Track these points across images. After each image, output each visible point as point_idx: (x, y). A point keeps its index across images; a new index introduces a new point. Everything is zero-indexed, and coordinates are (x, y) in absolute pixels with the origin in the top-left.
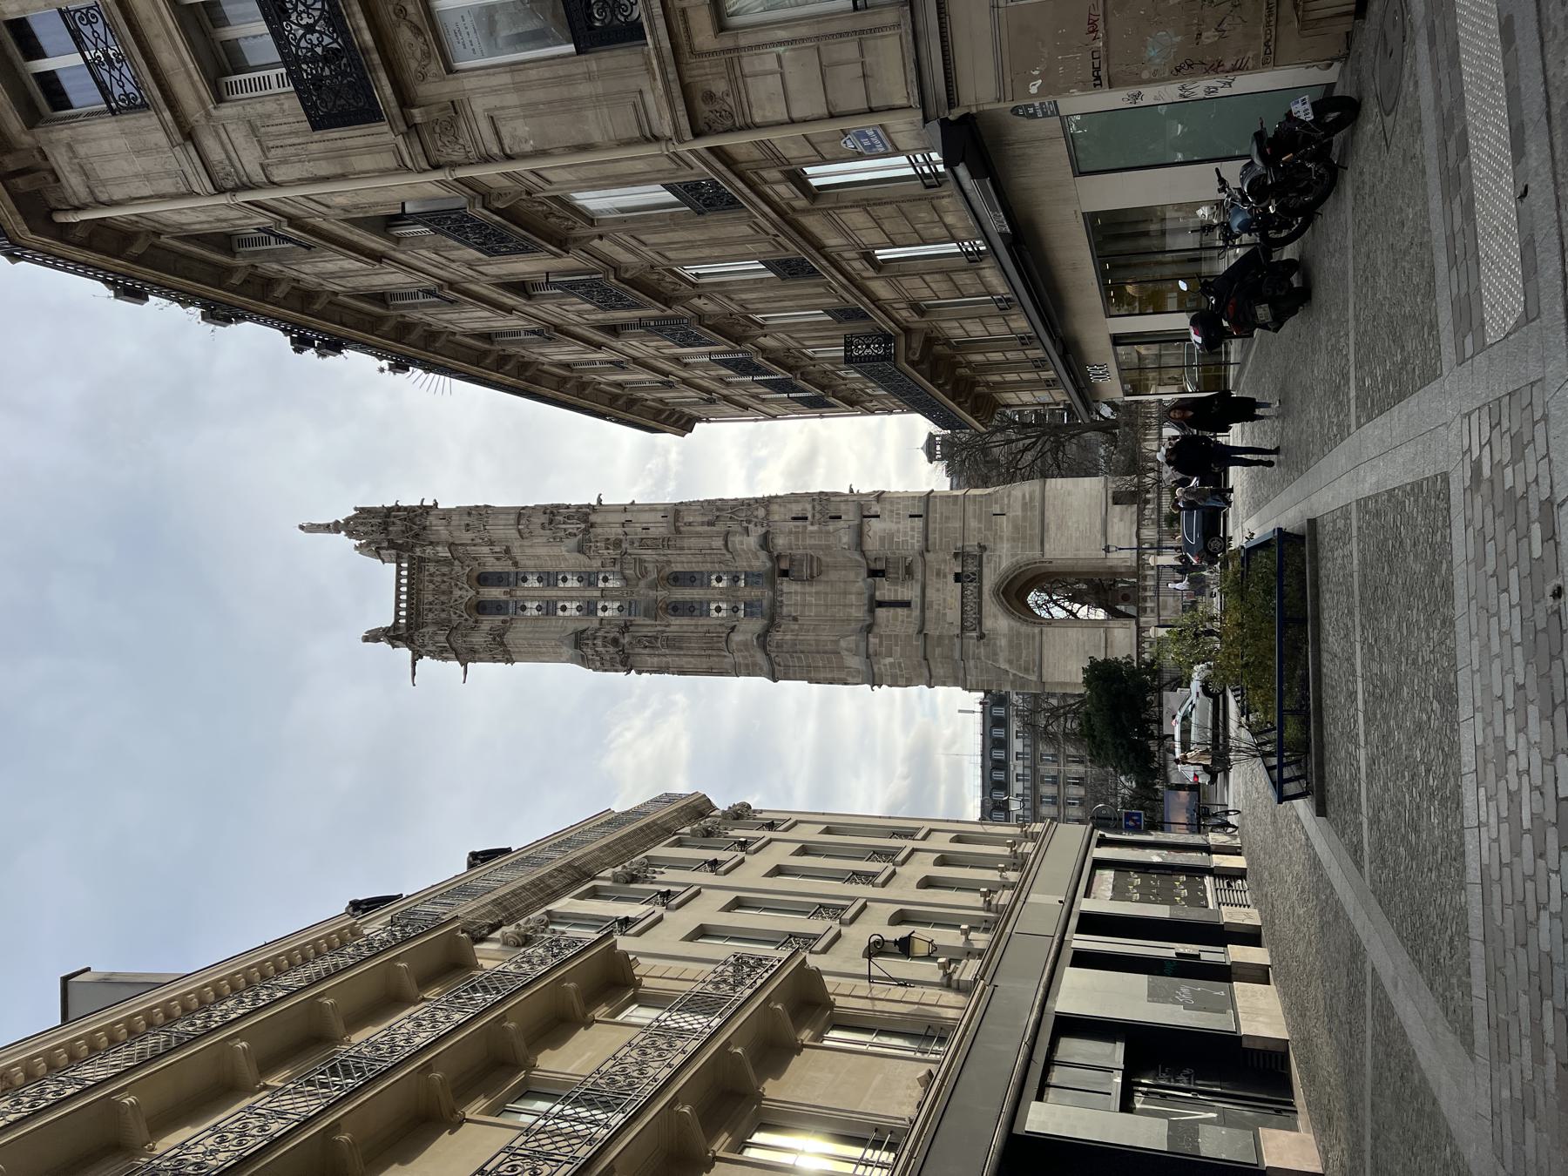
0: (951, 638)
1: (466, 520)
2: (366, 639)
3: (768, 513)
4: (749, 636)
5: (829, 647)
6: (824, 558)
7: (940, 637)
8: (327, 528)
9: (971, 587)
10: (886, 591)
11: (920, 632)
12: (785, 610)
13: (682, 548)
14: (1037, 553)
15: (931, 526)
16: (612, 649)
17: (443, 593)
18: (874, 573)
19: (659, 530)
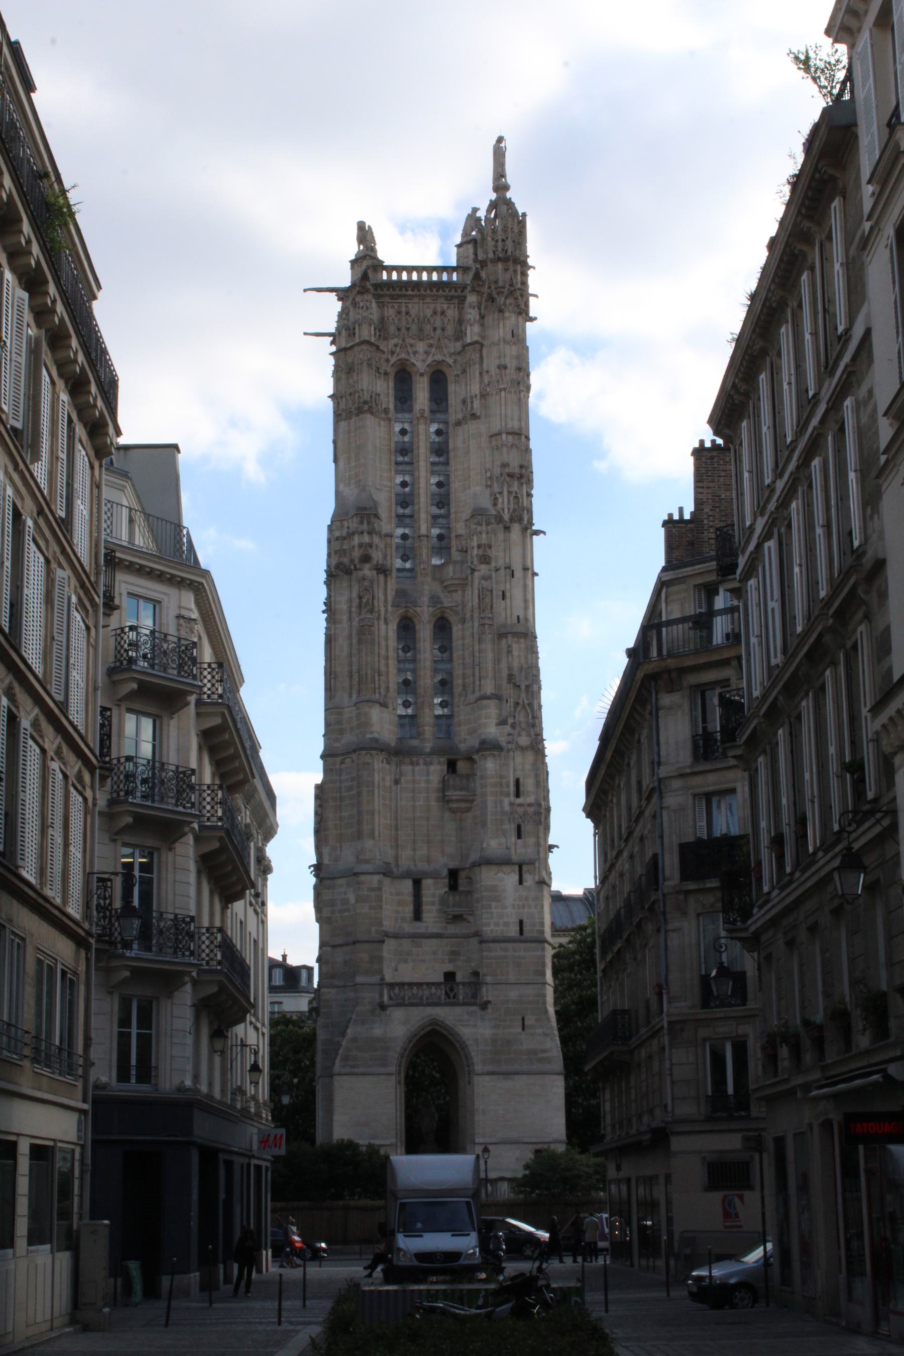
0: (380, 972)
1: (512, 364)
2: (361, 226)
3: (523, 749)
4: (376, 728)
5: (366, 827)
6: (470, 815)
7: (381, 959)
9: (441, 992)
10: (433, 891)
11: (387, 935)
12: (407, 768)
13: (480, 641)
14: (478, 1068)
15: (510, 946)
16: (357, 554)
17: (421, 330)
18: (453, 875)
19: (504, 613)
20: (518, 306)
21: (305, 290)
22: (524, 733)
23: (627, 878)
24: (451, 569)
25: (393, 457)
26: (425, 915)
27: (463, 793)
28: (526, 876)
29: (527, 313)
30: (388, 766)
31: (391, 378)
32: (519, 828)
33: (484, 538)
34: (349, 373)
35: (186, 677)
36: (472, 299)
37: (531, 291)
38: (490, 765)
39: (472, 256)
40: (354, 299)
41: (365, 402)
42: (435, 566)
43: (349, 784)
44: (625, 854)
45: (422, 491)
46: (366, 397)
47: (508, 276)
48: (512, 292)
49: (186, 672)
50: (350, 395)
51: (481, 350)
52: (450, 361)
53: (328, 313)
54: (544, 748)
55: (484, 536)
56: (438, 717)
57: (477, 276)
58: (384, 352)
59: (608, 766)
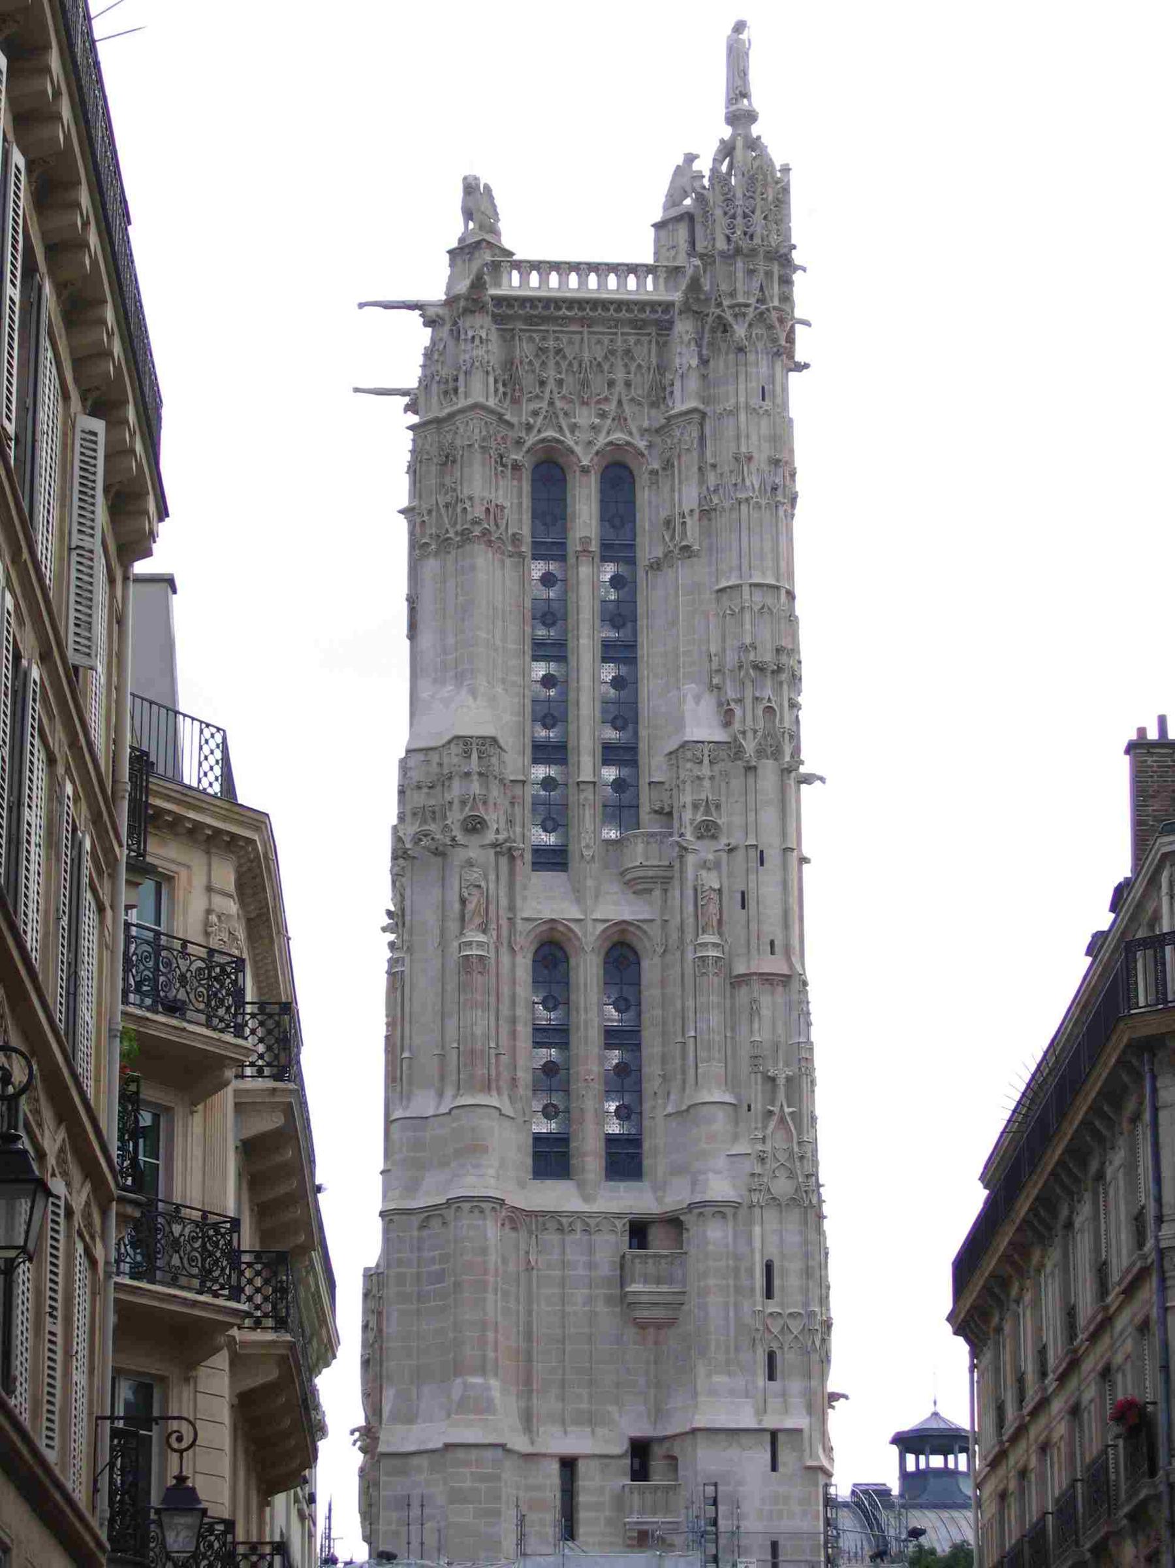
8: (738, 90)
16: (455, 817)
18: (640, 1450)
20: (775, 340)
21: (361, 305)
22: (782, 1174)
23: (1059, 1455)
24: (640, 847)
25: (528, 629)
26: (582, 1530)
27: (664, 1288)
28: (784, 1456)
29: (791, 356)
30: (513, 1235)
31: (526, 475)
32: (771, 1357)
33: (706, 792)
34: (444, 464)
35: (222, 1031)
36: (683, 328)
37: (798, 313)
38: (715, 1233)
39: (683, 246)
40: (455, 323)
41: (476, 522)
42: (608, 842)
43: (437, 1267)
44: (1057, 1405)
45: (585, 699)
46: (478, 512)
47: (756, 285)
48: (762, 314)
49: (222, 1020)
50: (447, 506)
51: (702, 425)
52: (641, 444)
53: (404, 350)
54: (821, 1201)
55: (707, 783)
56: (611, 1140)
57: (695, 285)
58: (510, 425)
59: (1018, 1230)
